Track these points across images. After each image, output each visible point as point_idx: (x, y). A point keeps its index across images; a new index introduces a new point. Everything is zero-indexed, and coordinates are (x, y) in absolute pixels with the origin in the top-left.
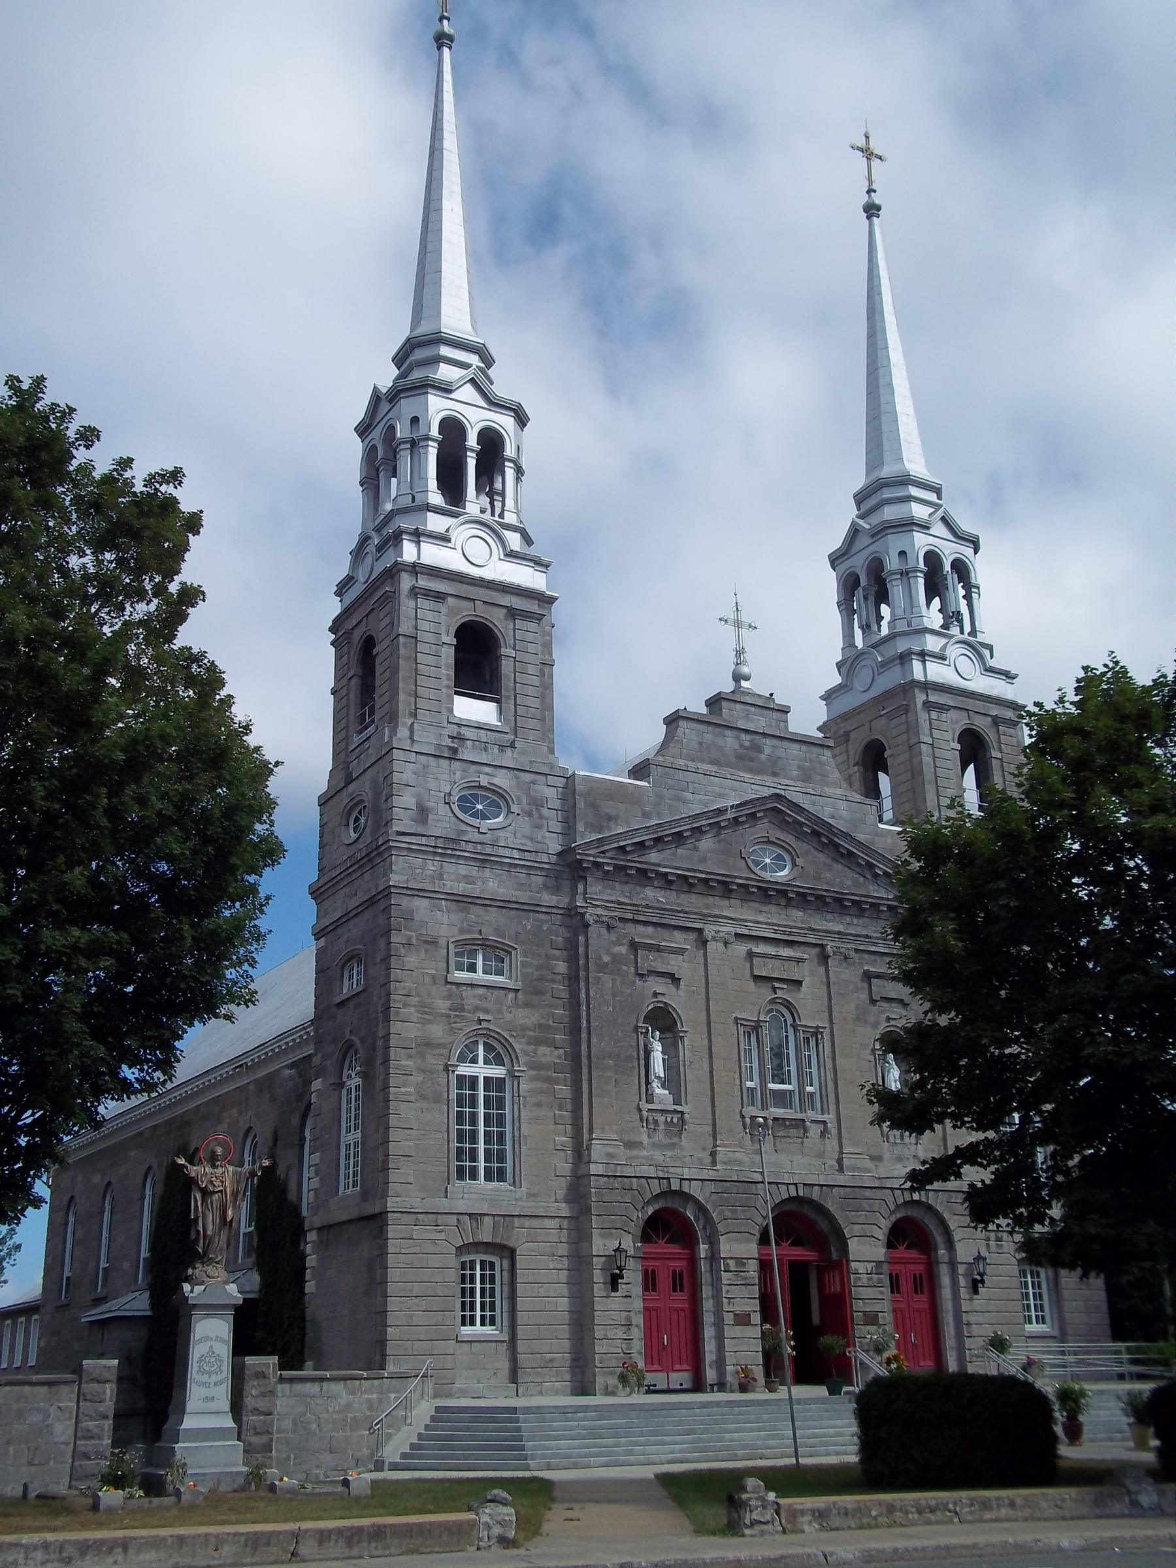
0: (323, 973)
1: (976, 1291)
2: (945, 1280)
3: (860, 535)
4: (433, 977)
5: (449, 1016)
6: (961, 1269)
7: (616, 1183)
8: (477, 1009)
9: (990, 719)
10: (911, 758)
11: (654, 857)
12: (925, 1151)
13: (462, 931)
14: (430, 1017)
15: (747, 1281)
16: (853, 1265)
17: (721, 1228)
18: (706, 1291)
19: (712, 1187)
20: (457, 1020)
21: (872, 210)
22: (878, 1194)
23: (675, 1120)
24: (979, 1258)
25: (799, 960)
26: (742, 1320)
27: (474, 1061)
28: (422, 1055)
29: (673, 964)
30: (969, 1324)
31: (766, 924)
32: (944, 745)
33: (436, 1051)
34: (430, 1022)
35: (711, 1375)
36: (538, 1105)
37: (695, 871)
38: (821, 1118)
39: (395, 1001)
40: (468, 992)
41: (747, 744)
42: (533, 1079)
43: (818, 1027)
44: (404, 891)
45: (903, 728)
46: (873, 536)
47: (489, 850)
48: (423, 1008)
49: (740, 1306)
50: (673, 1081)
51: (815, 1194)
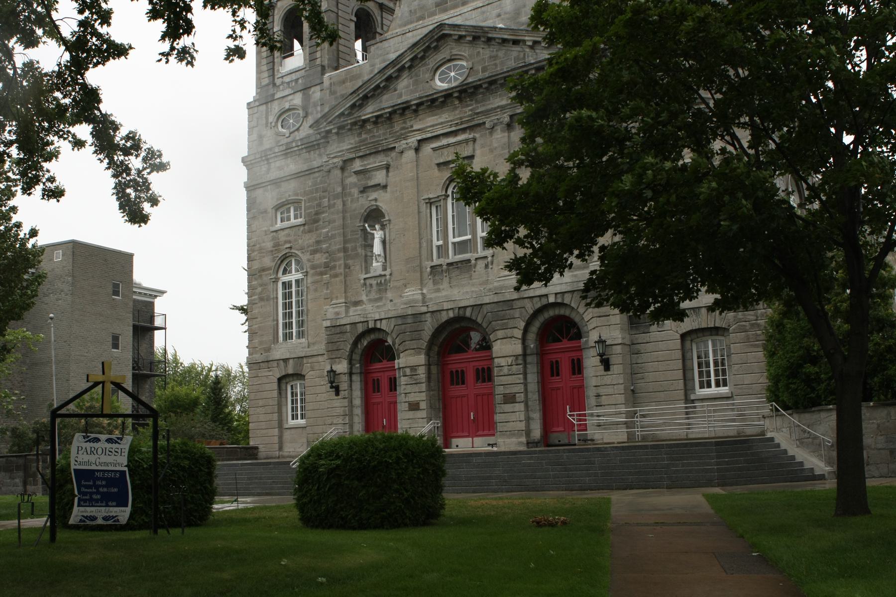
7: (338, 330)
8: (286, 242)
13: (278, 199)
22: (518, 304)
24: (601, 342)
25: (466, 141)
26: (414, 407)
27: (290, 272)
29: (379, 177)
30: (598, 396)
36: (316, 290)
37: (384, 109)
42: (314, 275)
48: (261, 249)
49: (412, 398)
51: (468, 313)
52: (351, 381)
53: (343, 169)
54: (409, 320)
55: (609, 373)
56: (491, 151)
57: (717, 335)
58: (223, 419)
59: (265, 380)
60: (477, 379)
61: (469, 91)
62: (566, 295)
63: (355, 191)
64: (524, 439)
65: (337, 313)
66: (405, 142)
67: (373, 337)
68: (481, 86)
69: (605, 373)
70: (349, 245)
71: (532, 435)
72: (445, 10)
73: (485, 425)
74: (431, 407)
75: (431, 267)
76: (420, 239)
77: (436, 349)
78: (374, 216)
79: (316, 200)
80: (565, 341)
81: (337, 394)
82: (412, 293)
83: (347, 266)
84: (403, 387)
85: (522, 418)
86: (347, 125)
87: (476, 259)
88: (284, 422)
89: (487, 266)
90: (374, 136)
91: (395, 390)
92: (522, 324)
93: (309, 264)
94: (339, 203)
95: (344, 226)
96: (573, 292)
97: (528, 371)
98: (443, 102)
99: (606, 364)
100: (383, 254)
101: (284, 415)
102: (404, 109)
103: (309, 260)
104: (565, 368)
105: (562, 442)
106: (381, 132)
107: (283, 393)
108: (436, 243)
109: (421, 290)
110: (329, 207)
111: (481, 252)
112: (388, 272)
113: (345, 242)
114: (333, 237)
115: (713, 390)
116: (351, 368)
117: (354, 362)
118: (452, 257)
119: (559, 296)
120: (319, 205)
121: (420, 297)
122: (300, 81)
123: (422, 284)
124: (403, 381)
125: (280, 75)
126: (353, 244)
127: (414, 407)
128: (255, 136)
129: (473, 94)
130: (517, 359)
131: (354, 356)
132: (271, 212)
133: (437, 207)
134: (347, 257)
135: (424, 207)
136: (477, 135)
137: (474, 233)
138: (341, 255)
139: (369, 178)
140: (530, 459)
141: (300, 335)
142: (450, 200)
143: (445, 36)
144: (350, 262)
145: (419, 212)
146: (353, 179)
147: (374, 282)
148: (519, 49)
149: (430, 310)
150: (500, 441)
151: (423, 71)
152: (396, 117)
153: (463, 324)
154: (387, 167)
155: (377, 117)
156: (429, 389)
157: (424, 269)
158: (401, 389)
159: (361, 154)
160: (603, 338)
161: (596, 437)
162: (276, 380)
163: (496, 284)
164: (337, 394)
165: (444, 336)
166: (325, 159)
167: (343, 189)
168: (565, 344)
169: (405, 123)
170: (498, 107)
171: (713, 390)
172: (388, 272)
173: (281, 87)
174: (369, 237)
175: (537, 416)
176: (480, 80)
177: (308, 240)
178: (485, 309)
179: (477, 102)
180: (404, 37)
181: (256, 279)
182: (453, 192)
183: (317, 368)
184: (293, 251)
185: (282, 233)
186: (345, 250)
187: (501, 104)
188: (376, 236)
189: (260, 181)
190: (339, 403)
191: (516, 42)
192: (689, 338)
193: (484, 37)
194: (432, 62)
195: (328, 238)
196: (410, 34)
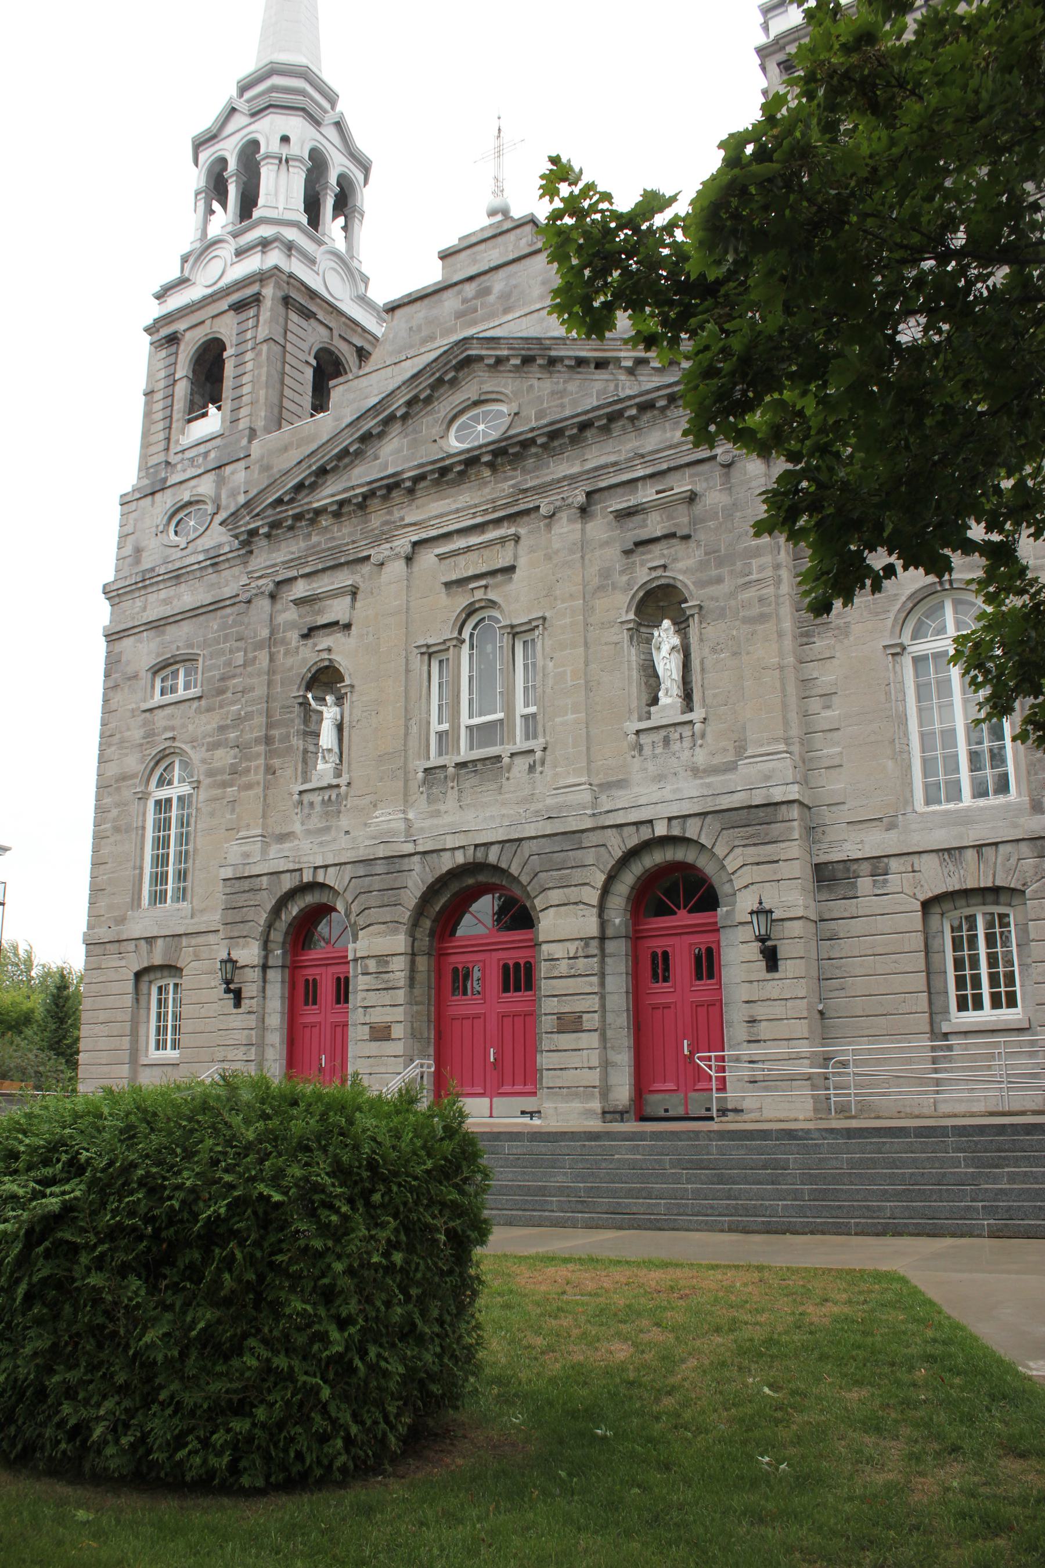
4: (133, 710)
7: (246, 885)
8: (166, 729)
13: (158, 655)
15: (390, 985)
19: (348, 871)
23: (334, 797)
24: (762, 912)
25: (502, 540)
26: (381, 1033)
27: (170, 783)
29: (338, 610)
30: (752, 1021)
33: (131, 782)
34: (126, 755)
36: (212, 814)
37: (353, 488)
42: (211, 786)
43: (530, 622)
47: (178, 565)
48: (122, 741)
49: (377, 1016)
52: (265, 981)
53: (273, 597)
54: (380, 868)
55: (776, 975)
56: (548, 557)
57: (997, 903)
58: (69, 1046)
59: (112, 975)
60: (506, 989)
61: (511, 451)
62: (690, 822)
63: (293, 636)
64: (596, 1105)
65: (247, 855)
66: (388, 546)
67: (309, 899)
68: (532, 441)
69: (769, 976)
70: (276, 733)
71: (612, 1096)
72: (475, 323)
73: (518, 1072)
74: (414, 1034)
75: (426, 770)
76: (408, 719)
77: (427, 924)
78: (325, 679)
79: (224, 654)
80: (682, 913)
81: (238, 1004)
82: (387, 819)
83: (270, 770)
84: (361, 995)
85: (595, 1062)
86: (286, 519)
87: (512, 755)
88: (142, 1053)
89: (532, 768)
90: (333, 538)
91: (347, 1001)
92: (600, 878)
93: (203, 768)
94: (263, 656)
95: (268, 699)
96: (704, 815)
97: (608, 970)
98: (461, 473)
99: (771, 958)
100: (336, 750)
101: (142, 1039)
102: (390, 488)
103: (204, 761)
104: (682, 966)
105: (671, 1113)
106: (345, 531)
107: (143, 999)
108: (435, 727)
109: (404, 812)
110: (245, 665)
111: (520, 743)
112: (343, 781)
113: (269, 726)
114: (249, 716)
115: (987, 1015)
116: (266, 957)
117: (271, 946)
118: (465, 753)
119: (674, 822)
120: (228, 663)
121: (401, 826)
122: (212, 455)
123: (407, 801)
124: (360, 983)
125: (180, 448)
126: (283, 731)
127: (381, 1033)
128: (128, 550)
129: (518, 457)
130: (587, 945)
131: (272, 937)
132: (145, 677)
133: (441, 662)
134: (270, 754)
135: (418, 663)
136: (522, 531)
137: (509, 707)
138: (261, 748)
139: (320, 612)
140: (635, 1150)
141: (182, 895)
142: (466, 647)
144: (276, 762)
145: (408, 671)
146: (291, 614)
147: (316, 798)
148: (606, 377)
149: (420, 849)
150: (548, 1106)
151: (428, 423)
152: (375, 503)
153: (482, 878)
154: (354, 592)
155: (341, 504)
156: (411, 1001)
157: (411, 776)
158: (356, 999)
159: (307, 570)
160: (767, 906)
161: (746, 1105)
162: (132, 976)
163: (549, 801)
164: (238, 1004)
165: (443, 900)
166: (245, 580)
167: (272, 633)
168: (683, 918)
169: (390, 513)
170: (565, 478)
171: (987, 1015)
172: (343, 781)
173: (179, 467)
174: (314, 717)
175: (623, 1058)
176: (532, 430)
177: (206, 724)
178: (527, 848)
179: (524, 471)
180: (396, 368)
181: (110, 794)
182: (472, 635)
183: (204, 956)
184: (177, 744)
185: (160, 713)
186: (268, 740)
187: (568, 472)
188: (326, 715)
190: (239, 1021)
192: (938, 910)
193: (542, 356)
194: (445, 405)
195: (239, 720)
196: (409, 362)
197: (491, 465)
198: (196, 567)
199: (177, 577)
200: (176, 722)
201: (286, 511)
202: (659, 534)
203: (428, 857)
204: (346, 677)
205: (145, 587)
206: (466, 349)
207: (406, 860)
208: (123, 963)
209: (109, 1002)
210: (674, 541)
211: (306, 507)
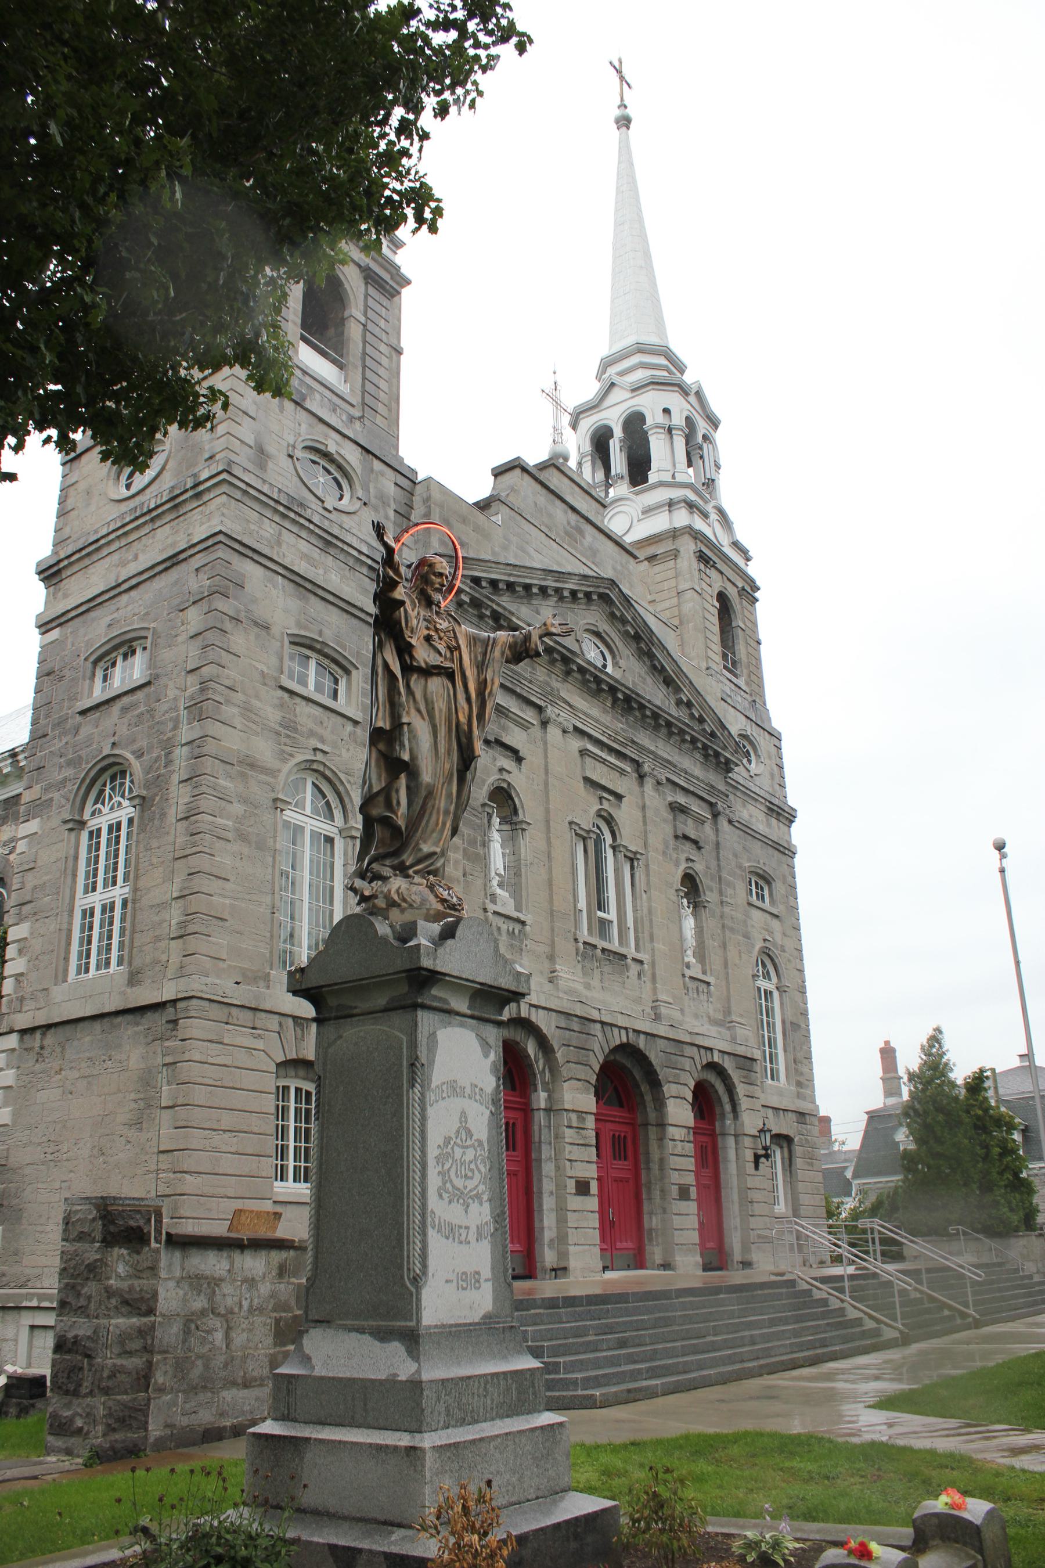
0: (47, 674)
1: (757, 1168)
2: (732, 1154)
3: (616, 390)
5: (278, 734)
6: (747, 1142)
8: (312, 734)
9: (736, 590)
10: (679, 605)
11: (505, 602)
12: (715, 1010)
14: (259, 730)
16: (671, 1131)
17: (565, 1072)
18: (546, 1152)
20: (287, 741)
21: (624, 122)
22: (690, 1051)
26: (582, 1188)
28: (243, 775)
29: (515, 737)
31: (597, 721)
32: (709, 599)
33: (263, 777)
34: (257, 734)
35: (548, 1257)
38: (639, 956)
39: (215, 691)
40: (304, 710)
41: (573, 523)
43: (635, 853)
44: (236, 546)
45: (671, 573)
46: (633, 390)
47: (336, 531)
48: (247, 710)
50: (514, 879)
51: (642, 1043)
54: (576, 1027)
55: (758, 1173)
59: (242, 1058)
68: (642, 707)
75: (585, 943)
143: (604, 598)
149: (604, 1019)
176: (649, 702)
179: (627, 723)
181: (229, 776)
189: (266, 551)
191: (668, 682)
197: (615, 700)
198: (355, 553)
199: (328, 543)
200: (326, 734)
201: (492, 601)
202: (693, 837)
203: (607, 1029)
204: (520, 812)
205: (284, 516)
206: (609, 589)
207: (592, 1025)
208: (260, 1044)
209: (238, 1099)
210: (694, 847)
211: (507, 614)
